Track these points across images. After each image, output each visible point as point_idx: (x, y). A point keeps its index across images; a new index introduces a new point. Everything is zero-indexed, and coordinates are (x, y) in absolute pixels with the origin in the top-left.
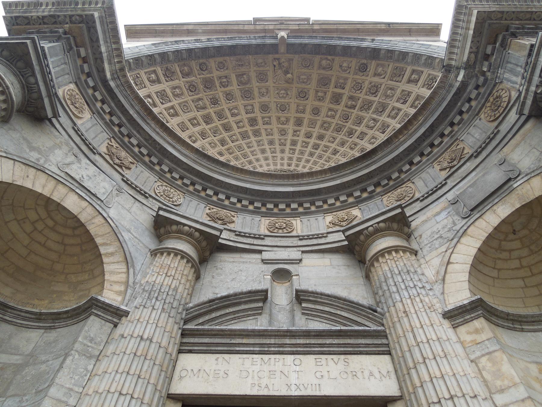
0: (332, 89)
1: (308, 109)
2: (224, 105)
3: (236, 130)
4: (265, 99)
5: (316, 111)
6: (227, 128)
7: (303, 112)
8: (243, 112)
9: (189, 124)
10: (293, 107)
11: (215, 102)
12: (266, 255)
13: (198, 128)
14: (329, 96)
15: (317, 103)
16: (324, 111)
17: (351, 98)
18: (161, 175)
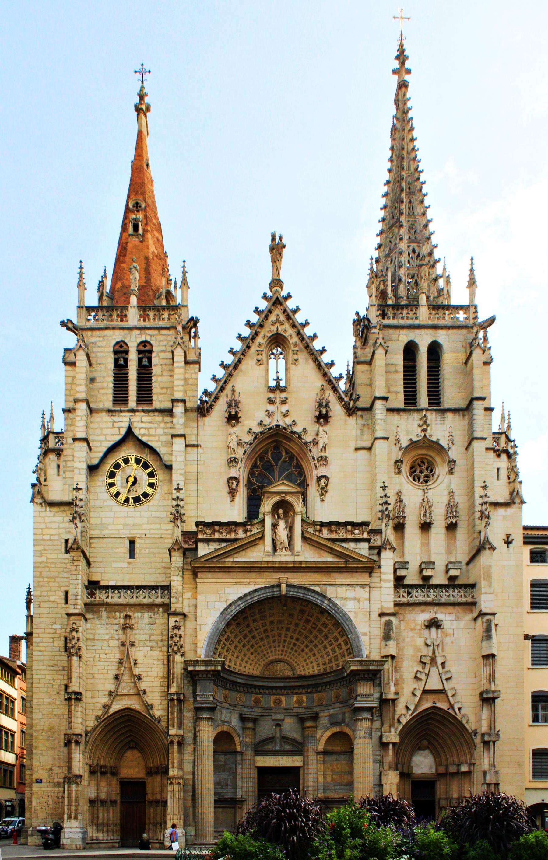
0: (306, 616)
1: (293, 623)
2: (253, 626)
3: (258, 637)
4: (273, 618)
5: (297, 625)
6: (254, 637)
7: (291, 624)
8: (261, 627)
9: (238, 644)
10: (286, 622)
11: (248, 626)
12: (274, 717)
13: (242, 644)
14: (304, 619)
15: (298, 621)
16: (301, 626)
17: (315, 624)
18: (237, 691)
